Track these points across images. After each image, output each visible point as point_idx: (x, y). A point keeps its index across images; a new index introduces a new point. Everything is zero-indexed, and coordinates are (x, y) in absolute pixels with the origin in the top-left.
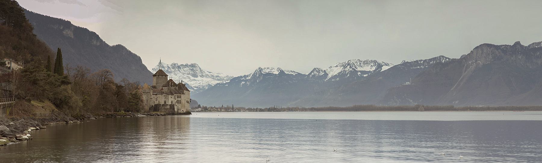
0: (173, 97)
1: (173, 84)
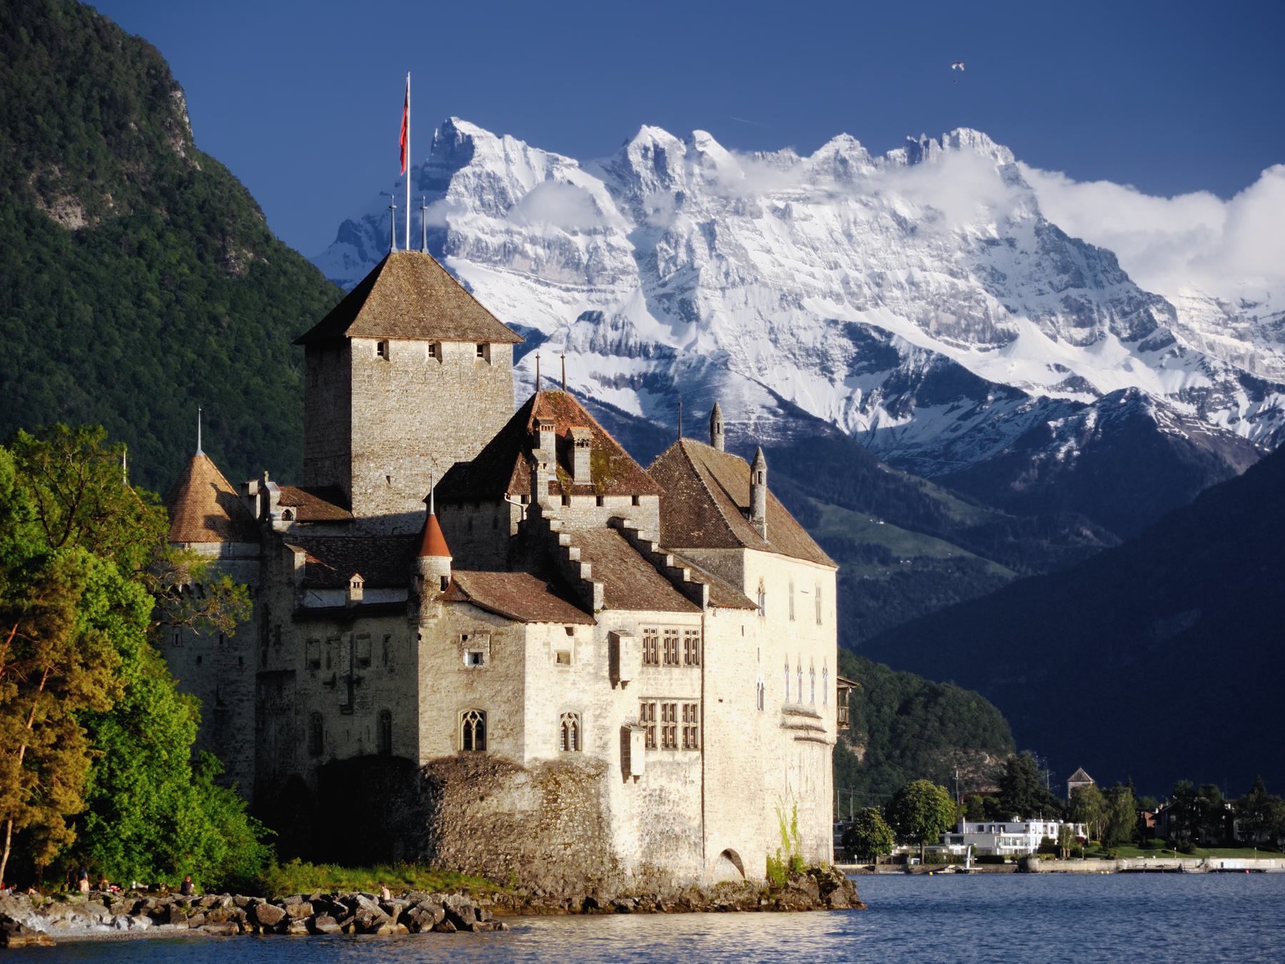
1: (582, 460)
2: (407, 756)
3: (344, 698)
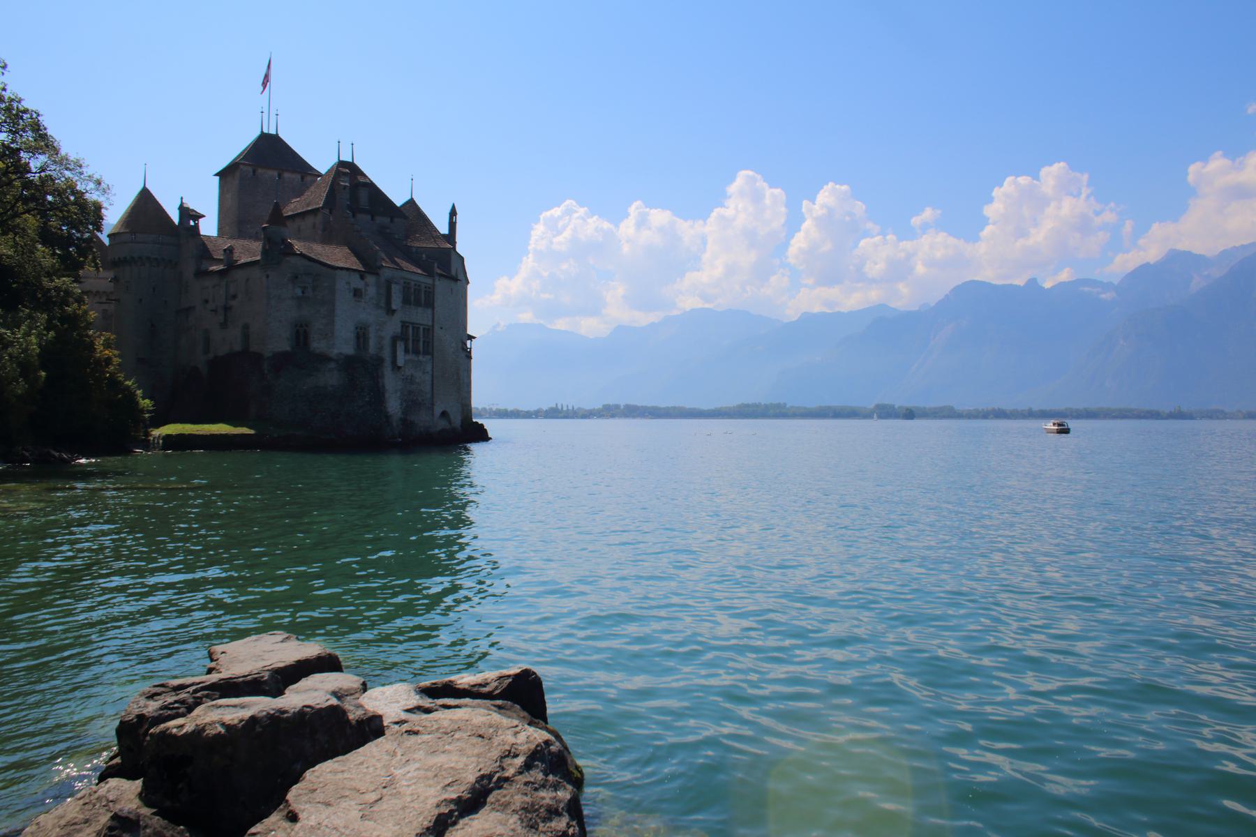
0: (372, 291)
3: (221, 318)
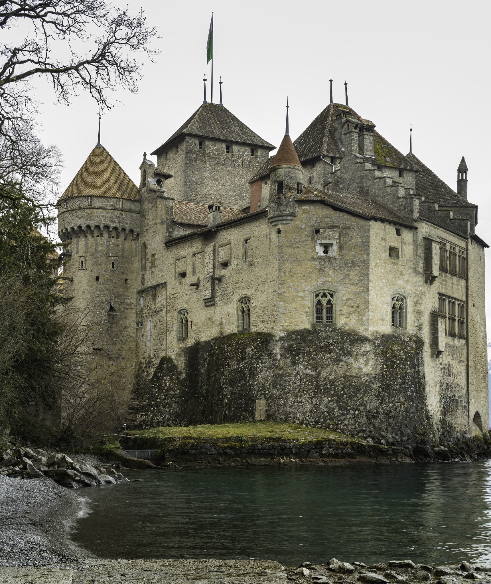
2: (265, 331)
